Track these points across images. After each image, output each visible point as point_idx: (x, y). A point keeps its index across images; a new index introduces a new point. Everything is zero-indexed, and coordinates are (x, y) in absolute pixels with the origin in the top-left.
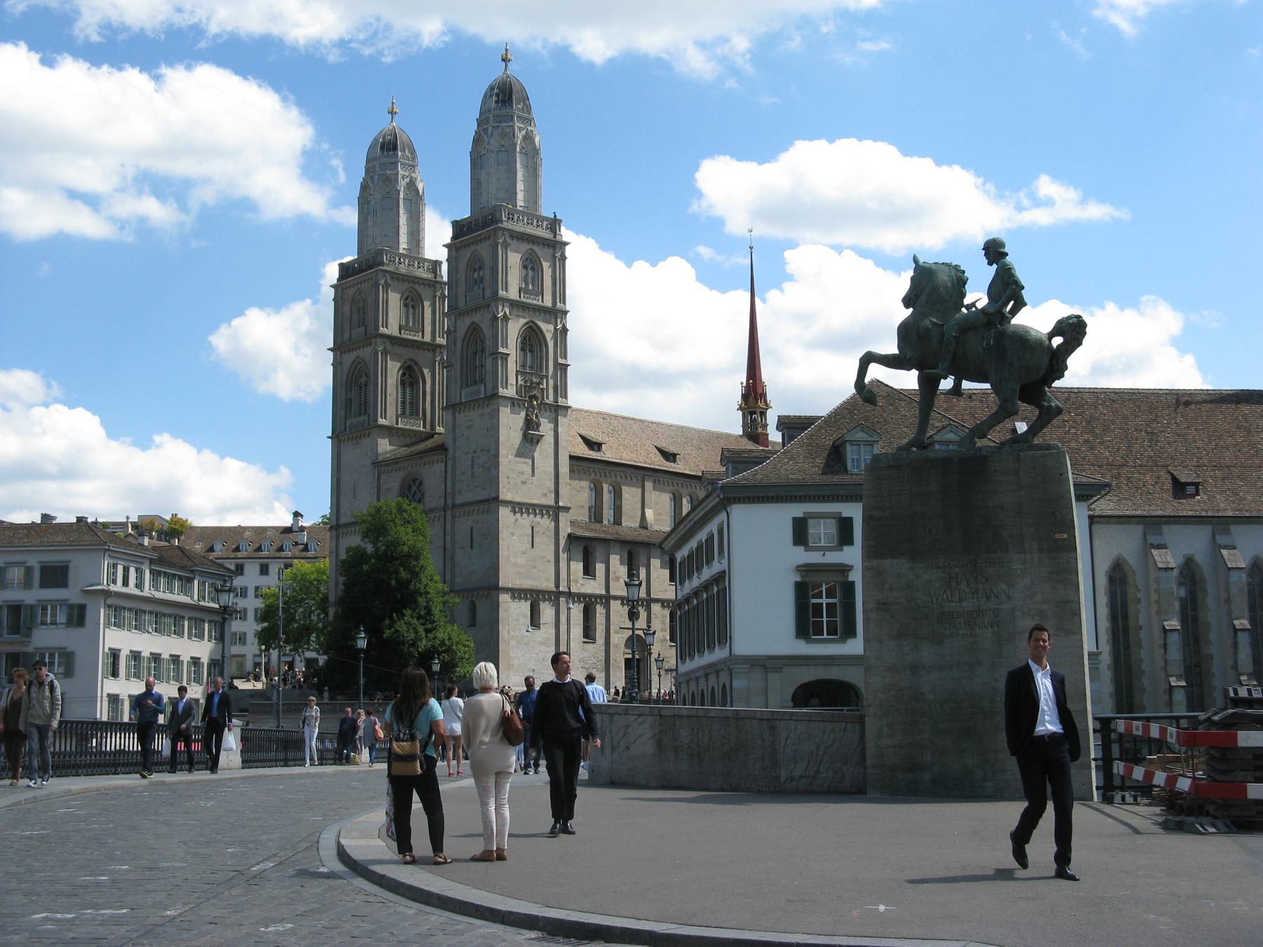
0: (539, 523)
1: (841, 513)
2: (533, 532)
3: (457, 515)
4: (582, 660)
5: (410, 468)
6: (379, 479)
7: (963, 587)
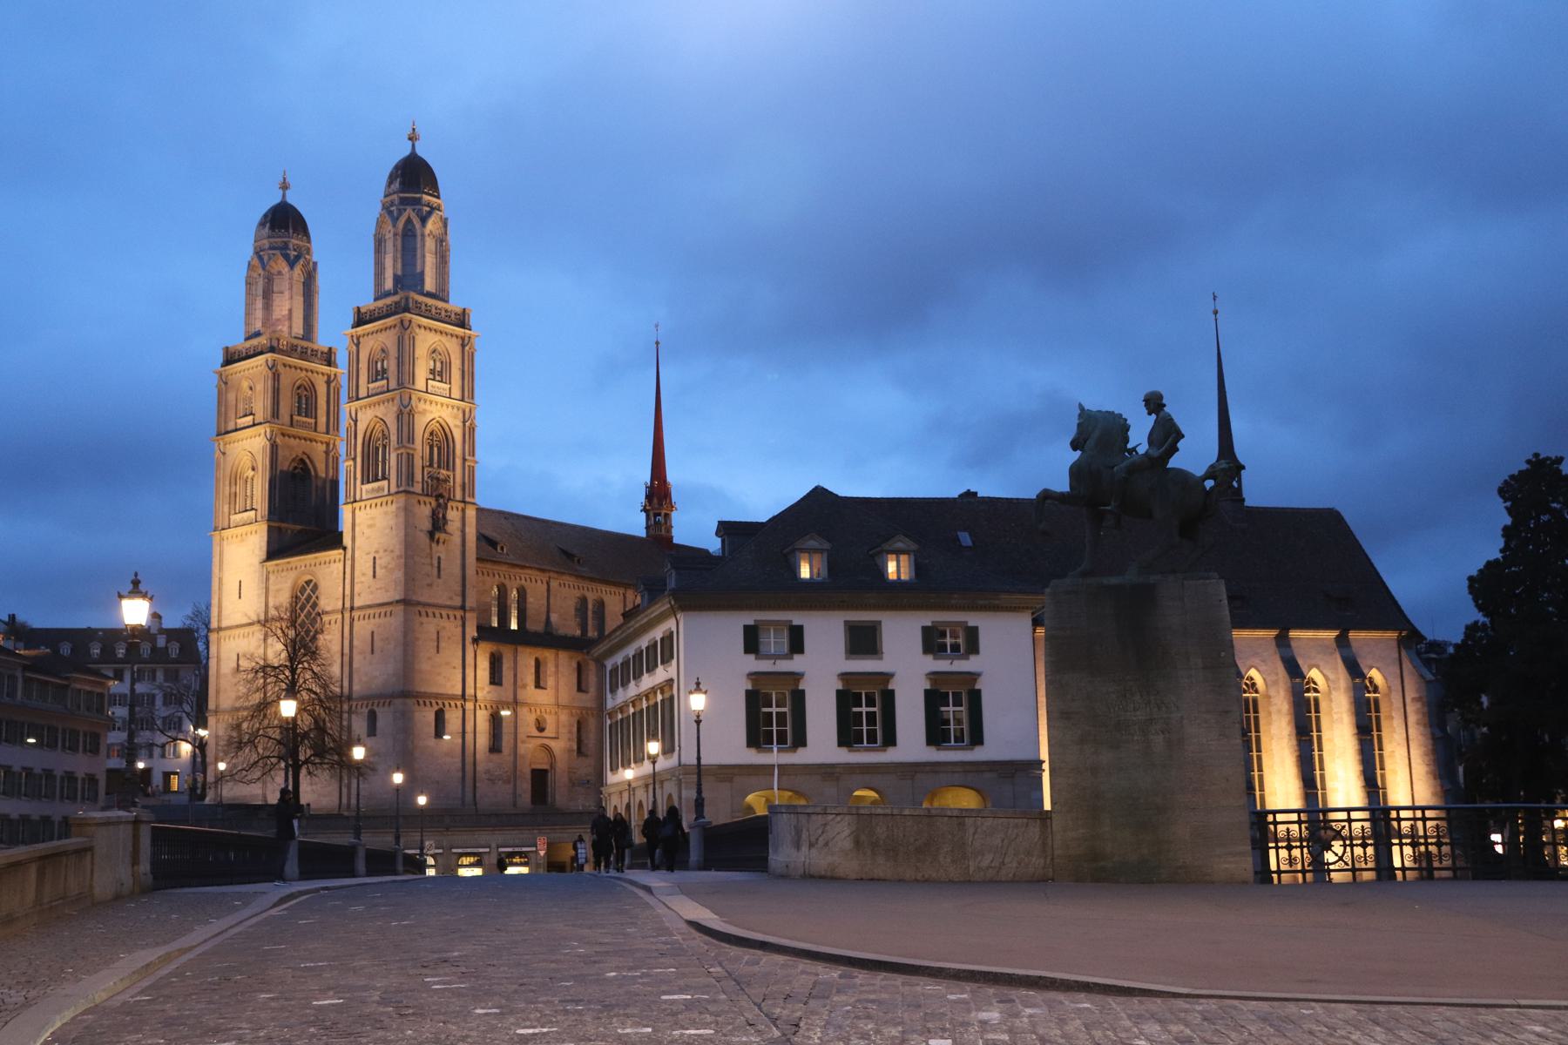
0: (444, 628)
1: (791, 621)
2: (438, 638)
3: (356, 618)
4: (487, 772)
5: (303, 568)
6: (267, 579)
7: (1137, 698)
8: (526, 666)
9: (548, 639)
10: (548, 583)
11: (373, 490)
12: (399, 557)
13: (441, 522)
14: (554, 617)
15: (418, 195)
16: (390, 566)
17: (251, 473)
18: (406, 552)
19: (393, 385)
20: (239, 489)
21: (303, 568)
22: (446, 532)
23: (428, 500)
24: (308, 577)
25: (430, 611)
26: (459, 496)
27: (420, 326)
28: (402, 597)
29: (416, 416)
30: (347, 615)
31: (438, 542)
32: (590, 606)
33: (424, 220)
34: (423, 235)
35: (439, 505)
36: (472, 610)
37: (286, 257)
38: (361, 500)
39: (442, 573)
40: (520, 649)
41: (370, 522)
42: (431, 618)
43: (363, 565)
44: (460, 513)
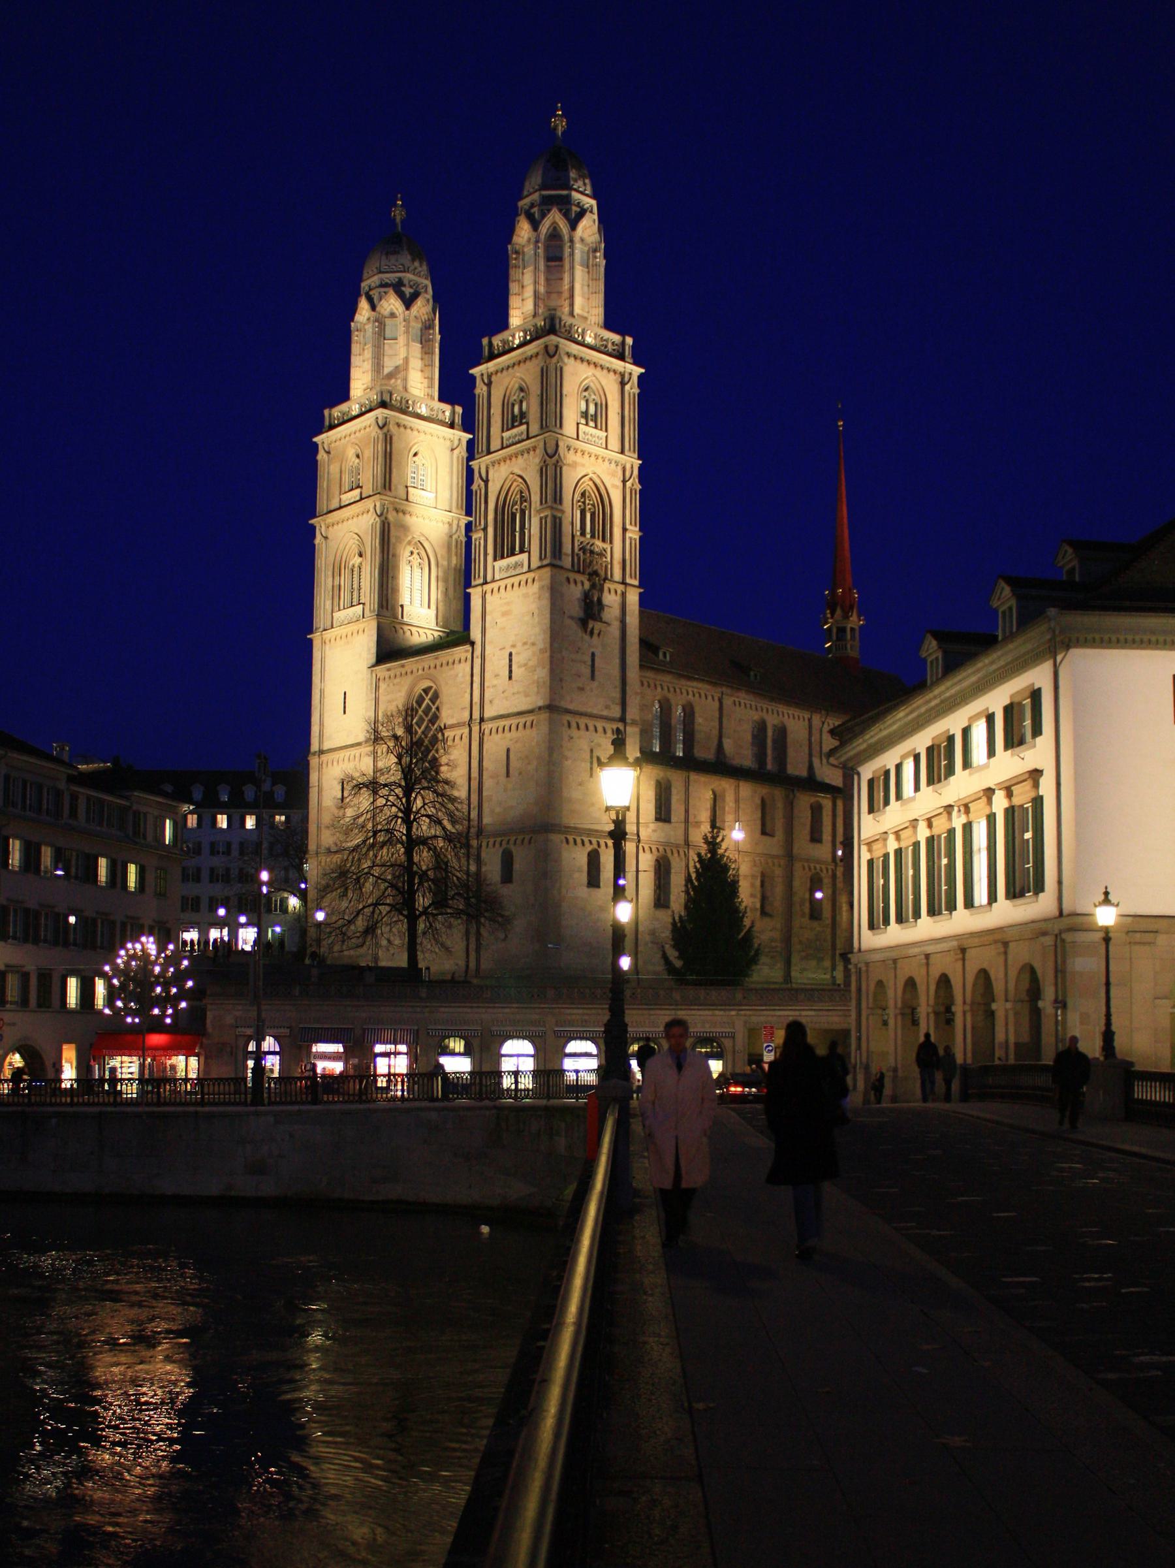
3: (487, 732)
5: (420, 672)
6: (377, 688)
8: (700, 799)
9: (720, 767)
10: (720, 701)
11: (508, 568)
12: (542, 651)
13: (596, 609)
14: (728, 744)
15: (565, 192)
16: (531, 663)
17: (357, 560)
18: (551, 645)
19: (535, 428)
20: (344, 581)
21: (420, 672)
22: (601, 620)
23: (579, 578)
24: (426, 684)
25: (583, 721)
26: (617, 576)
27: (569, 355)
28: (547, 703)
29: (564, 468)
30: (476, 729)
31: (592, 633)
32: (770, 733)
33: (573, 225)
34: (571, 241)
35: (593, 586)
36: (634, 723)
37: (401, 295)
38: (493, 581)
39: (597, 673)
40: (693, 776)
41: (504, 609)
42: (582, 732)
43: (496, 663)
44: (618, 598)
